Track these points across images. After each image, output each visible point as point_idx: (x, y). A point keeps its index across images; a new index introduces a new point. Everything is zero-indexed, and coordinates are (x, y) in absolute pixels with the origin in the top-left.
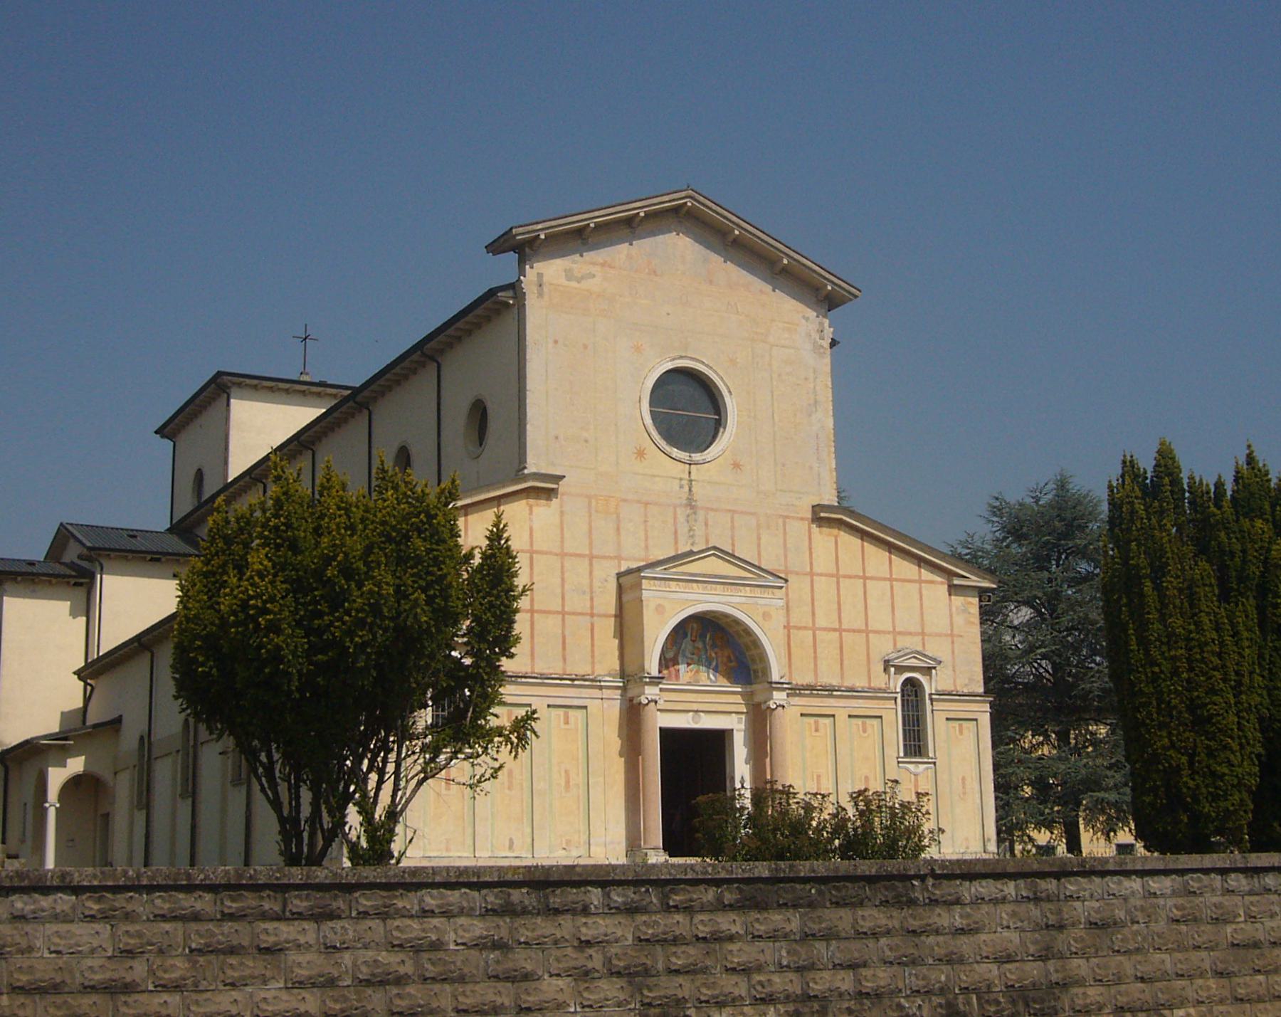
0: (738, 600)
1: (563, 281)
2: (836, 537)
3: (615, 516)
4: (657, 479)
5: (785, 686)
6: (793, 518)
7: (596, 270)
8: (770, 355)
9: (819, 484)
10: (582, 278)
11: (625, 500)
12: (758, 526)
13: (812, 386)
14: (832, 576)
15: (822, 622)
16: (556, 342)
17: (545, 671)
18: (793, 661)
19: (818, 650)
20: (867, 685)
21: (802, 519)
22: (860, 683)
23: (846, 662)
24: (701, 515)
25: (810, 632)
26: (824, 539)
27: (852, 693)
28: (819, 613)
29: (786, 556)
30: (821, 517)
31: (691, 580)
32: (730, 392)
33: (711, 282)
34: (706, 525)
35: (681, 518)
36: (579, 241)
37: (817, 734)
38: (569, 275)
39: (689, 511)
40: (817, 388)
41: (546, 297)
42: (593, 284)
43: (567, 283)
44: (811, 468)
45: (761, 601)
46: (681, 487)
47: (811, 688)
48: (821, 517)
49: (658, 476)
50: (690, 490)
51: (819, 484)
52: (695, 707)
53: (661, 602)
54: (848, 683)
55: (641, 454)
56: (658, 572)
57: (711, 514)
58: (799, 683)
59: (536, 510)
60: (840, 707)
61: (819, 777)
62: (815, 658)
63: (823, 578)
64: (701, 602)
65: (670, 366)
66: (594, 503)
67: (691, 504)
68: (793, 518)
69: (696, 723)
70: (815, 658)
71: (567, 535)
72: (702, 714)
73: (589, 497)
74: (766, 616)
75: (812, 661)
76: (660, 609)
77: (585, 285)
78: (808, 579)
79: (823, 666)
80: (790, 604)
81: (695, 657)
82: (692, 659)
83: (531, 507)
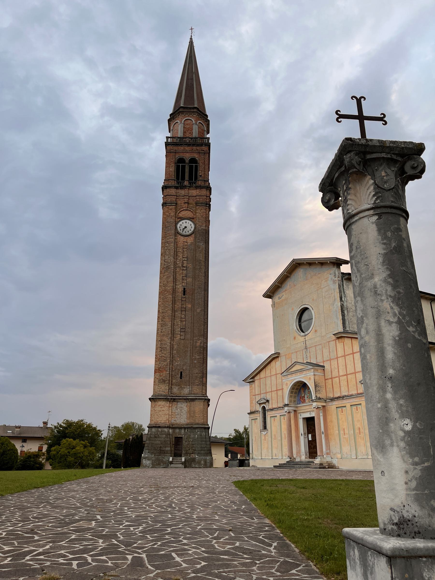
0: (304, 376)
1: (278, 301)
2: (343, 342)
3: (290, 358)
4: (298, 344)
5: (314, 401)
6: (331, 341)
7: (284, 293)
8: (322, 292)
9: (338, 326)
10: (282, 297)
11: (292, 353)
12: (322, 348)
13: (333, 295)
14: (343, 356)
15: (341, 374)
16: (278, 317)
17: (280, 406)
18: (334, 389)
19: (341, 383)
20: (356, 393)
21: (333, 340)
22: (354, 392)
23: (349, 386)
24: (308, 349)
25: (338, 378)
26: (340, 345)
27: (350, 396)
28: (340, 371)
29: (330, 355)
30: (339, 337)
31: (292, 373)
32: (313, 309)
33: (307, 280)
34: (310, 352)
35: (304, 353)
36: (280, 288)
37: (342, 414)
38: (279, 298)
39: (306, 350)
40: (335, 295)
41: (275, 307)
42: (283, 298)
43: (279, 300)
44: (335, 322)
45: (308, 374)
46: (304, 344)
47: (339, 397)
48: (339, 337)
49: (299, 343)
50: (306, 344)
51: (338, 326)
52: (309, 410)
53: (286, 382)
54: (350, 394)
55: (295, 338)
56: (285, 374)
57: (311, 348)
58: (336, 397)
59: (276, 363)
60: (347, 403)
61: (344, 429)
62: (340, 387)
63: (340, 358)
64: (295, 379)
65: (299, 310)
66: (286, 356)
67: (306, 348)
68: (331, 341)
69: (311, 415)
70: (340, 387)
71: (282, 367)
72: (311, 412)
73: (285, 355)
74: (310, 379)
75: (339, 388)
76: (287, 384)
77: (282, 299)
78: (336, 360)
79: (343, 389)
80: (332, 370)
81: (309, 394)
82: (308, 395)
83: (275, 362)
